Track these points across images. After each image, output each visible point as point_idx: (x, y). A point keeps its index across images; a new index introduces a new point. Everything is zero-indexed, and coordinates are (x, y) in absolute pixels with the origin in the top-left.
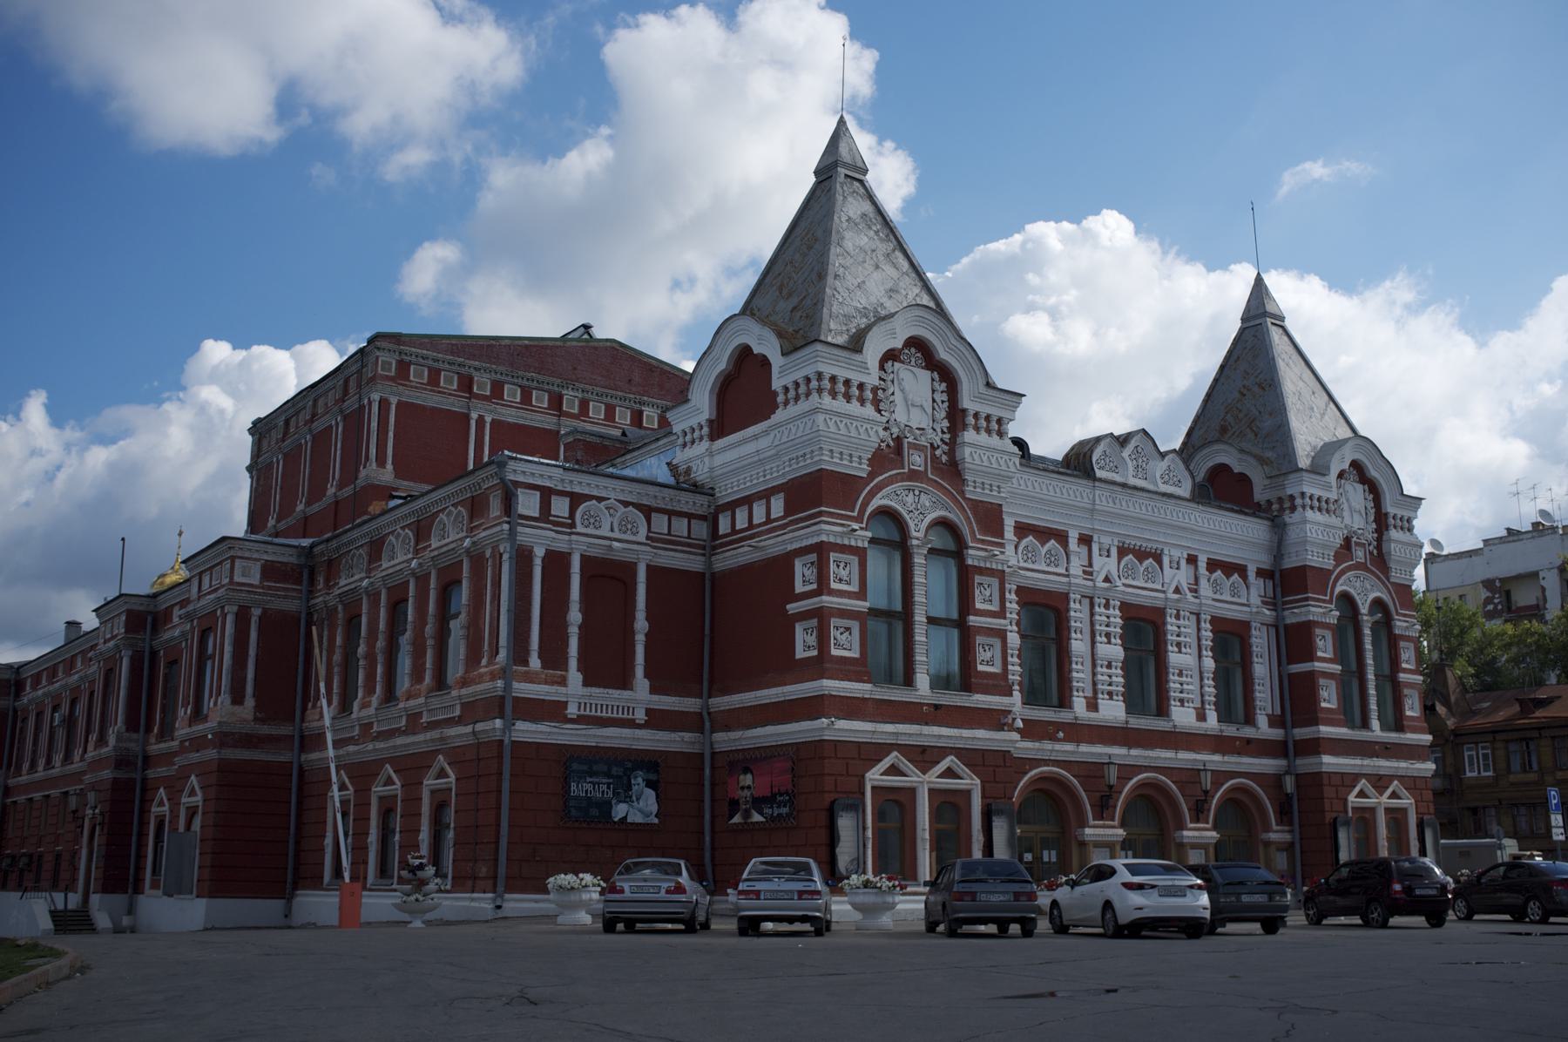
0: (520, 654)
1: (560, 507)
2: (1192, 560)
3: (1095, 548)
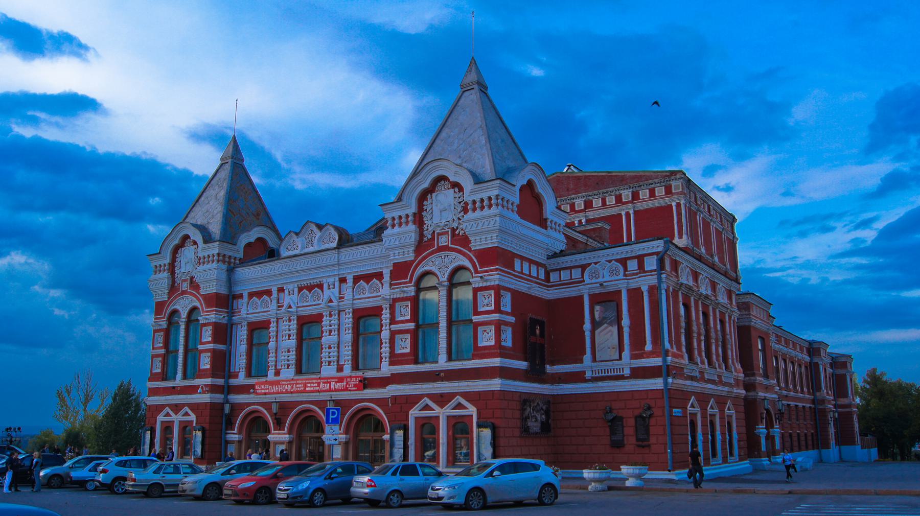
2: (343, 280)
3: (286, 292)
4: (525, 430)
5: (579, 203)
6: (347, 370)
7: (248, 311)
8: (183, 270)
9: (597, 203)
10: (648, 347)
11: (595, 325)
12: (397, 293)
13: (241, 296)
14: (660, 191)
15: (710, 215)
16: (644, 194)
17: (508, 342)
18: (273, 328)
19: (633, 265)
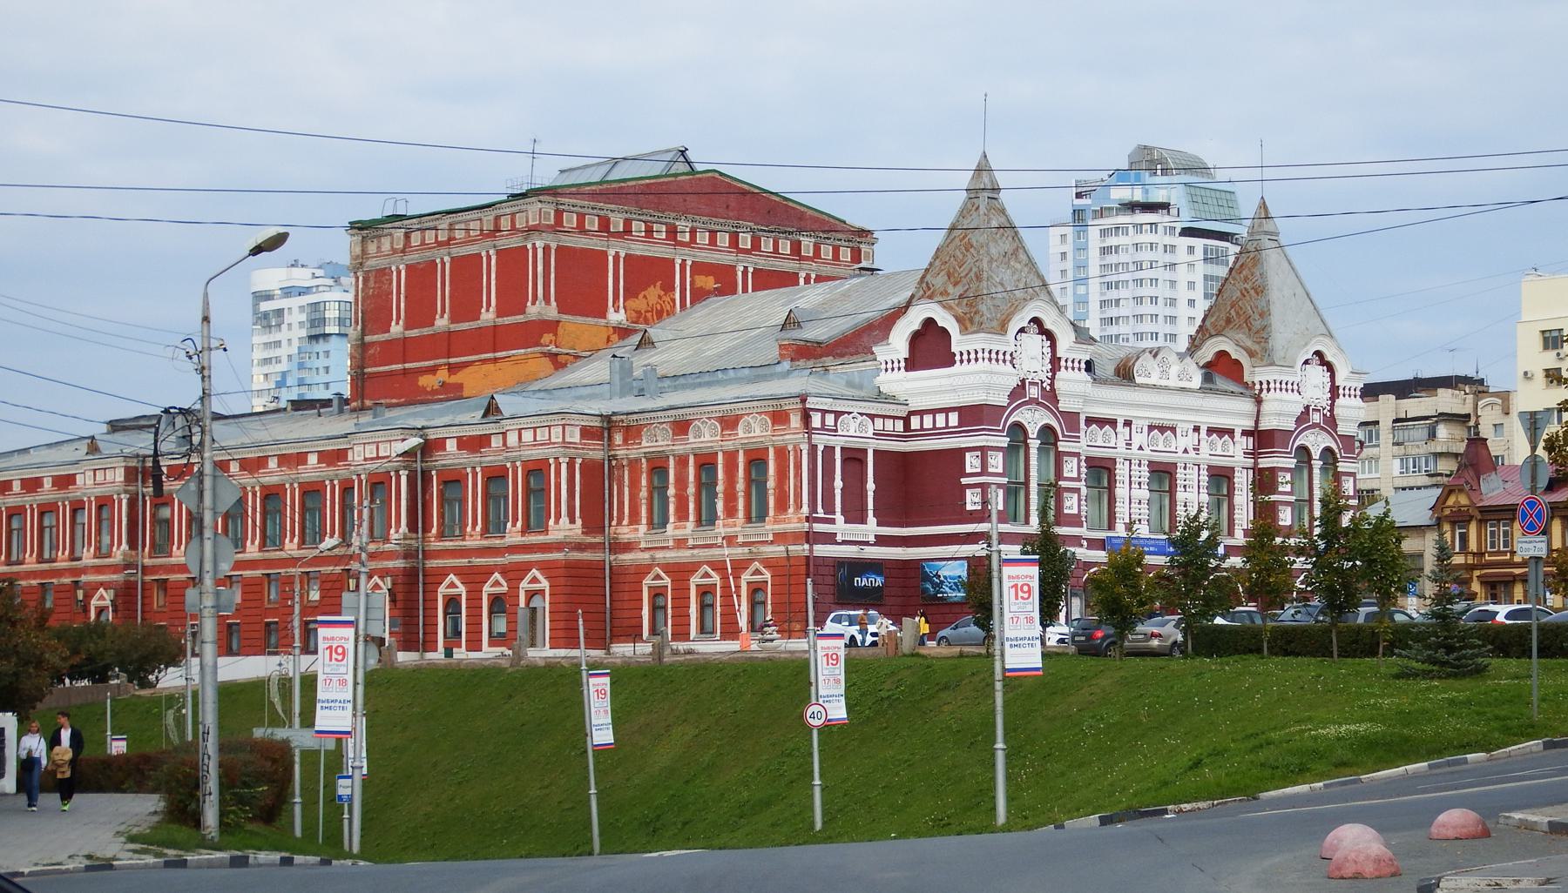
2: (1197, 429)
9: (767, 245)
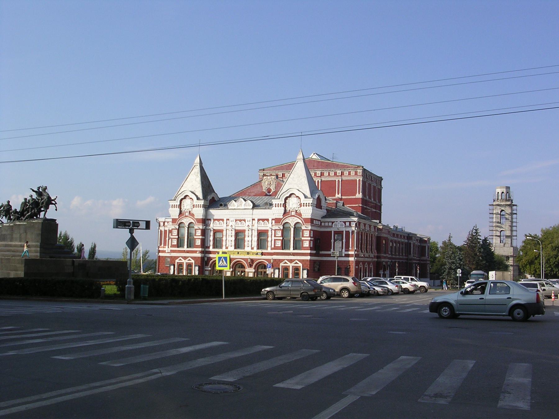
0: (161, 244)
1: (166, 224)
2: (253, 220)
4: (314, 270)
5: (318, 173)
6: (255, 248)
7: (213, 225)
8: (185, 208)
9: (326, 174)
10: (350, 249)
11: (335, 240)
12: (277, 228)
13: (210, 220)
14: (353, 173)
15: (372, 181)
16: (346, 173)
17: (312, 246)
18: (224, 233)
19: (348, 224)
